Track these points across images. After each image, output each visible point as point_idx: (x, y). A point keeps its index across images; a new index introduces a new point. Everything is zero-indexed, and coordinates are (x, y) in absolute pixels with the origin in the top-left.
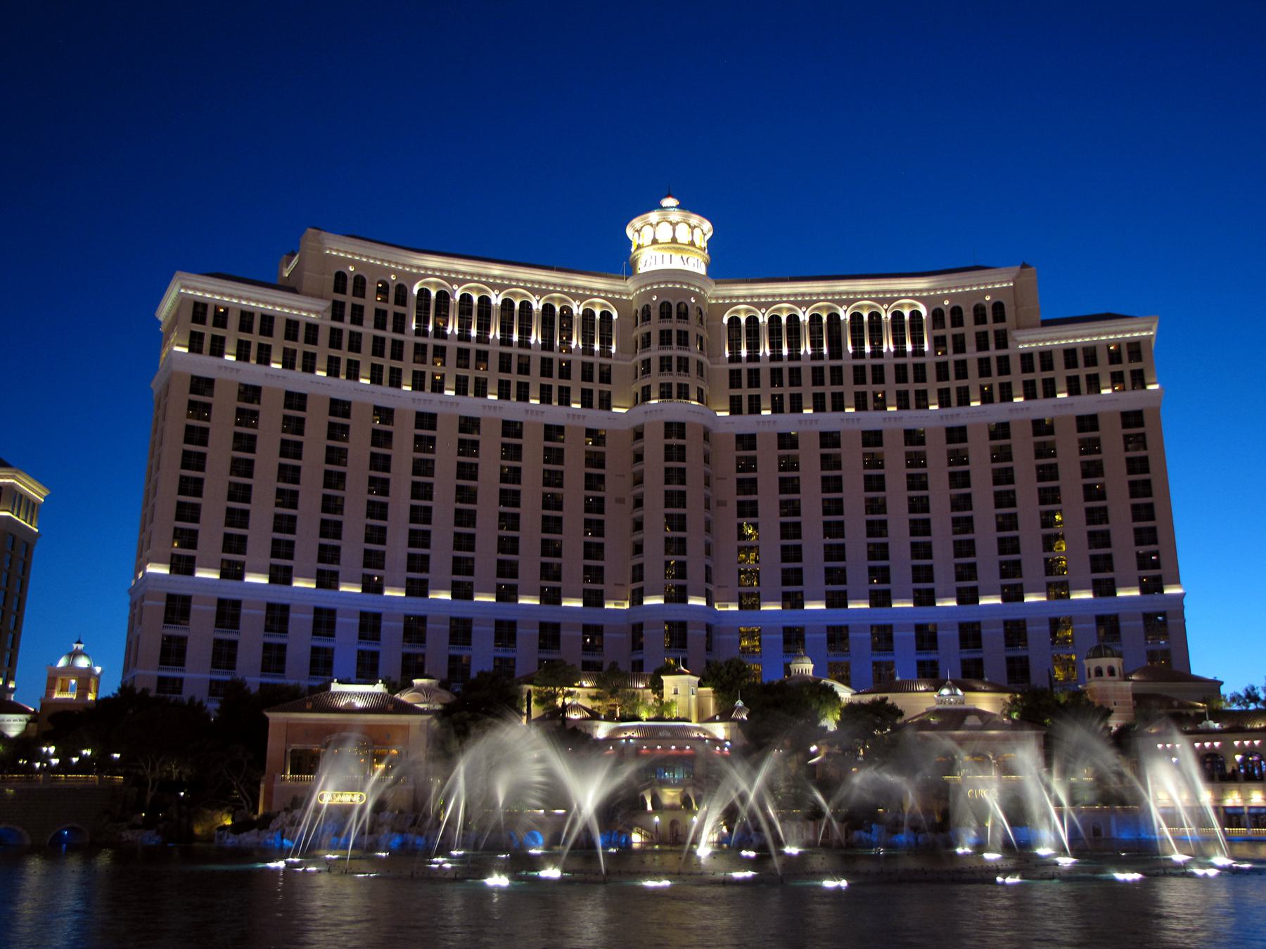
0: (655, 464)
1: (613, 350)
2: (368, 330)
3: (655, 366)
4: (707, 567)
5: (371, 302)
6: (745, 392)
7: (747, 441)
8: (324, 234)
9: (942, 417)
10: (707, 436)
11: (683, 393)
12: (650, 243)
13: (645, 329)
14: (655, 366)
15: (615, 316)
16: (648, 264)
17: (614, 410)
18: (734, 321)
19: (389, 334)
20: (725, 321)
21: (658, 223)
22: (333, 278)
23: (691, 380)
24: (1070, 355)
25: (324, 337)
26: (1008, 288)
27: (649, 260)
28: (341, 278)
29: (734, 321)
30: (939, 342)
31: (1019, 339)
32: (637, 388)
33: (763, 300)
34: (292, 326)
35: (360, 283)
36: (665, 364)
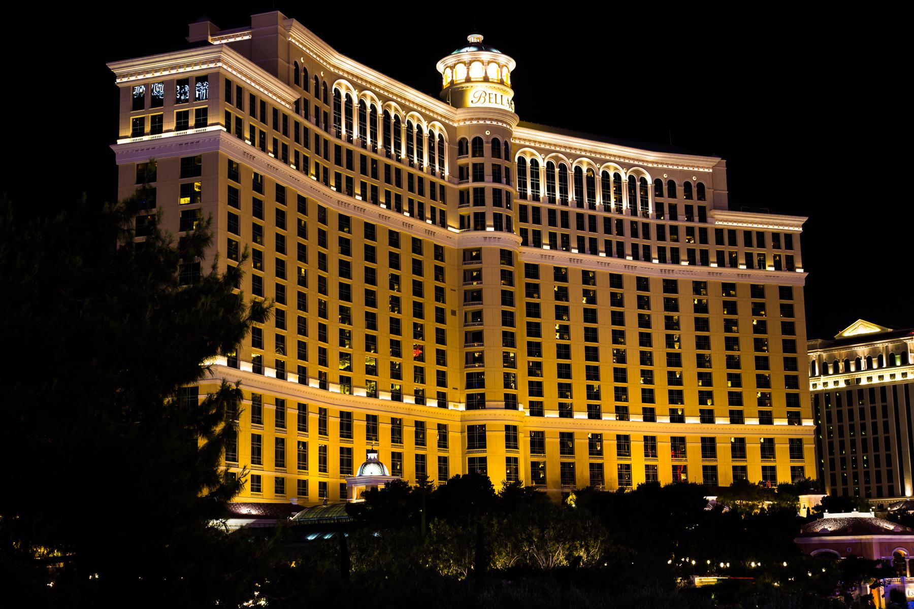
0: (492, 286)
1: (447, 173)
3: (489, 197)
8: (296, 23)
9: (661, 270)
12: (482, 79)
13: (478, 160)
14: (489, 197)
16: (482, 100)
17: (449, 228)
20: (516, 160)
21: (489, 63)
24: (748, 234)
26: (708, 173)
27: (475, 97)
29: (522, 161)
30: (659, 207)
31: (716, 216)
32: (469, 210)
33: (543, 146)
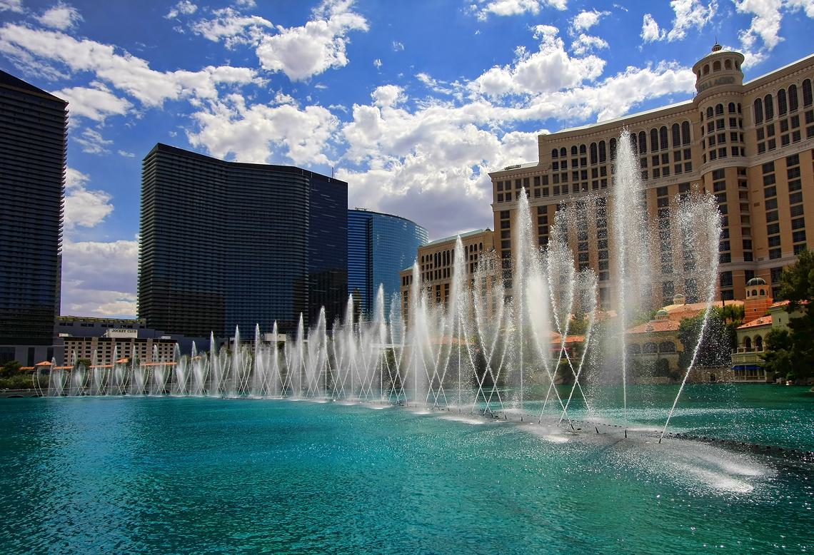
2: (570, 168)
4: (744, 242)
5: (569, 158)
6: (766, 139)
7: (769, 167)
10: (742, 171)
11: (723, 153)
15: (690, 122)
18: (758, 102)
19: (579, 168)
22: (551, 152)
23: (728, 145)
25: (551, 179)
28: (555, 153)
34: (537, 179)
35: (564, 151)
36: (712, 141)
